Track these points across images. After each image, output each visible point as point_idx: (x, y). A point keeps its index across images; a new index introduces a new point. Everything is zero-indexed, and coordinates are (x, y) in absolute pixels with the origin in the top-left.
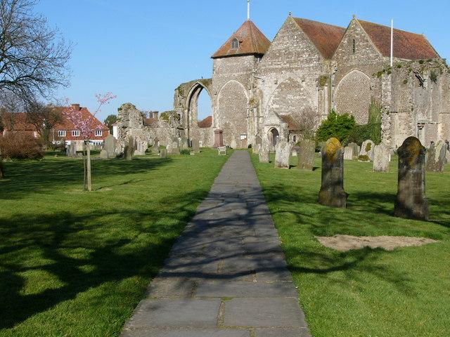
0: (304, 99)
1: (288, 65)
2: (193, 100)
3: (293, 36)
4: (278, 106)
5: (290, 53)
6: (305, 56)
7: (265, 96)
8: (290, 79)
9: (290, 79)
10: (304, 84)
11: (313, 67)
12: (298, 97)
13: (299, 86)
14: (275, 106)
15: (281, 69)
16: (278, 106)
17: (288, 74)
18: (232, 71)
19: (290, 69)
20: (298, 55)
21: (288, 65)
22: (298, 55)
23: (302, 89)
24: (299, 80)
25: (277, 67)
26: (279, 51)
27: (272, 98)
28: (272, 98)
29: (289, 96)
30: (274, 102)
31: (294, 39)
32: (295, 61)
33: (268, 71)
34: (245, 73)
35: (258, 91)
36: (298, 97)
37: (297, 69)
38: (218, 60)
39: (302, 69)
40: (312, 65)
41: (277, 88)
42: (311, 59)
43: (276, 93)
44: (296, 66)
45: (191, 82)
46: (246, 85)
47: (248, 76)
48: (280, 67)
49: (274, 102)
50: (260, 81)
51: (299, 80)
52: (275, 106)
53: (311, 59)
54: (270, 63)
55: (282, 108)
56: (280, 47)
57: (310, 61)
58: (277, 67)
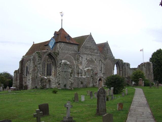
5: (91, 49)
6: (96, 51)
8: (91, 58)
9: (91, 58)
12: (93, 66)
13: (94, 62)
15: (88, 54)
20: (94, 50)
22: (94, 50)
24: (94, 60)
27: (85, 65)
28: (85, 65)
34: (74, 52)
35: (80, 61)
36: (93, 66)
37: (93, 55)
38: (62, 43)
39: (95, 55)
41: (87, 61)
42: (98, 53)
46: (74, 58)
50: (81, 58)
51: (94, 60)
54: (84, 51)
56: (88, 45)
57: (97, 53)
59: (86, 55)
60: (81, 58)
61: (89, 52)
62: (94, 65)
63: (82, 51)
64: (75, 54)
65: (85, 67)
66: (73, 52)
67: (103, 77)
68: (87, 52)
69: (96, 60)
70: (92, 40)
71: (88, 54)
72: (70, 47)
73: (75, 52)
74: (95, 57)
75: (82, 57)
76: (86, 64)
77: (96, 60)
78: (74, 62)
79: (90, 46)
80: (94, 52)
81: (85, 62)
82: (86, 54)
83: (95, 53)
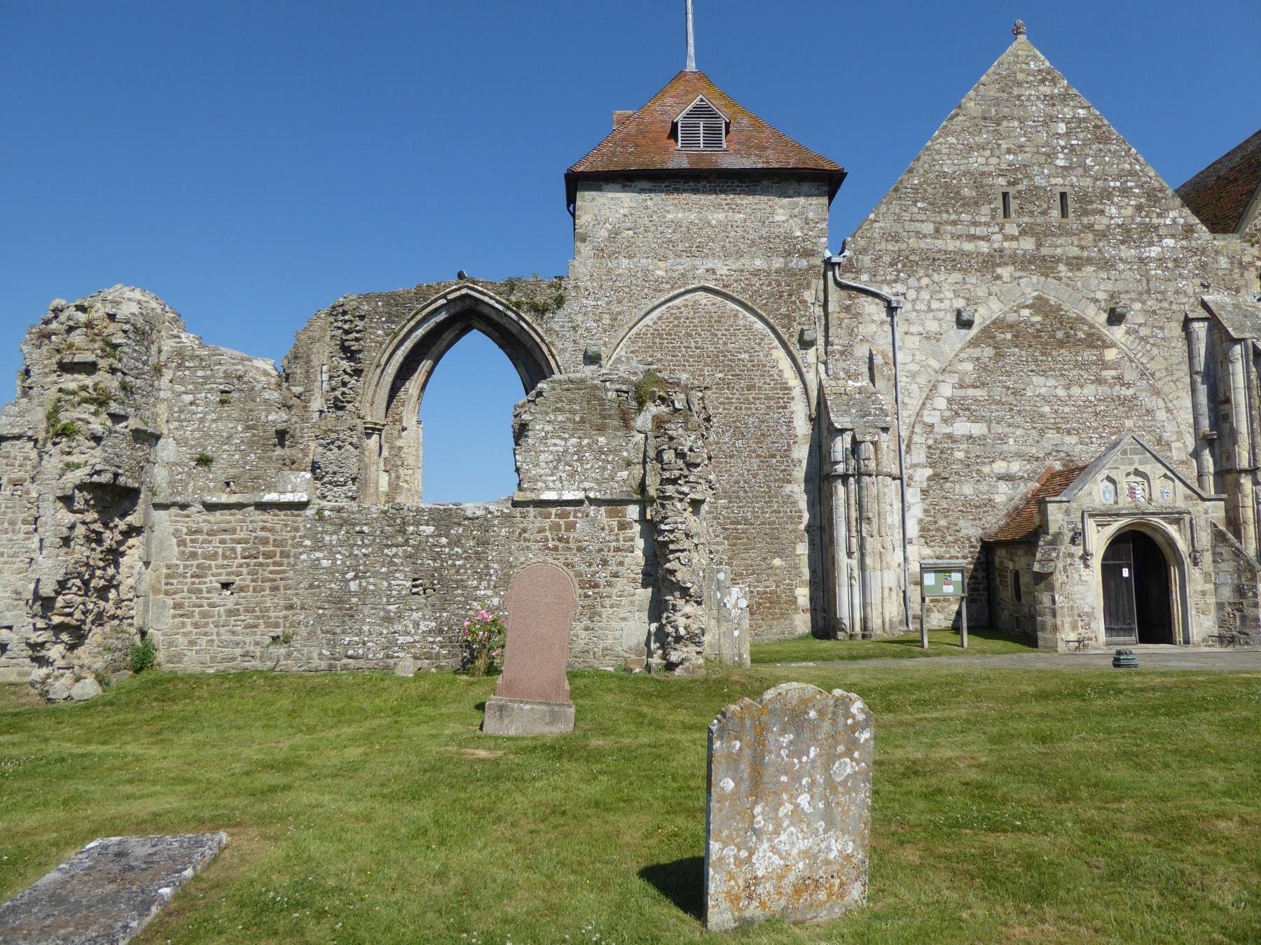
0: (1123, 401)
1: (1028, 244)
2: (412, 386)
3: (1053, 119)
4: (978, 429)
5: (1035, 191)
6: (1116, 213)
7: (903, 381)
8: (1040, 305)
9: (1040, 305)
10: (1118, 333)
11: (1161, 260)
12: (1090, 391)
13: (1095, 341)
14: (962, 427)
15: (990, 263)
16: (978, 429)
17: (1031, 286)
18: (696, 251)
19: (1045, 265)
21: (1028, 244)
23: (1111, 354)
25: (968, 246)
26: (978, 180)
28: (946, 390)
29: (1040, 385)
30: (959, 408)
31: (1059, 136)
32: (1064, 232)
33: (907, 264)
34: (778, 263)
37: (1076, 264)
39: (1106, 264)
40: (1154, 251)
41: (974, 343)
42: (1148, 229)
43: (968, 367)
44: (1075, 251)
45: (421, 294)
47: (798, 280)
48: (984, 247)
49: (959, 408)
52: (962, 427)
53: (1148, 229)
54: (928, 228)
55: (1002, 439)
56: (977, 161)
58: (968, 246)
59: (956, 276)
60: (874, 309)
61: (1013, 238)
62: (1099, 381)
63: (896, 238)
64: (798, 280)
65: (941, 403)
66: (759, 263)
67: (1176, 518)
68: (974, 238)
69: (1115, 318)
70: (1050, 100)
71: (990, 263)
72: (717, 217)
73: (788, 254)
74: (1099, 285)
75: (891, 310)
76: (963, 375)
77: (1115, 318)
78: (785, 364)
79: (1014, 173)
80: (1090, 227)
81: (935, 355)
82: (954, 262)
83: (1103, 235)
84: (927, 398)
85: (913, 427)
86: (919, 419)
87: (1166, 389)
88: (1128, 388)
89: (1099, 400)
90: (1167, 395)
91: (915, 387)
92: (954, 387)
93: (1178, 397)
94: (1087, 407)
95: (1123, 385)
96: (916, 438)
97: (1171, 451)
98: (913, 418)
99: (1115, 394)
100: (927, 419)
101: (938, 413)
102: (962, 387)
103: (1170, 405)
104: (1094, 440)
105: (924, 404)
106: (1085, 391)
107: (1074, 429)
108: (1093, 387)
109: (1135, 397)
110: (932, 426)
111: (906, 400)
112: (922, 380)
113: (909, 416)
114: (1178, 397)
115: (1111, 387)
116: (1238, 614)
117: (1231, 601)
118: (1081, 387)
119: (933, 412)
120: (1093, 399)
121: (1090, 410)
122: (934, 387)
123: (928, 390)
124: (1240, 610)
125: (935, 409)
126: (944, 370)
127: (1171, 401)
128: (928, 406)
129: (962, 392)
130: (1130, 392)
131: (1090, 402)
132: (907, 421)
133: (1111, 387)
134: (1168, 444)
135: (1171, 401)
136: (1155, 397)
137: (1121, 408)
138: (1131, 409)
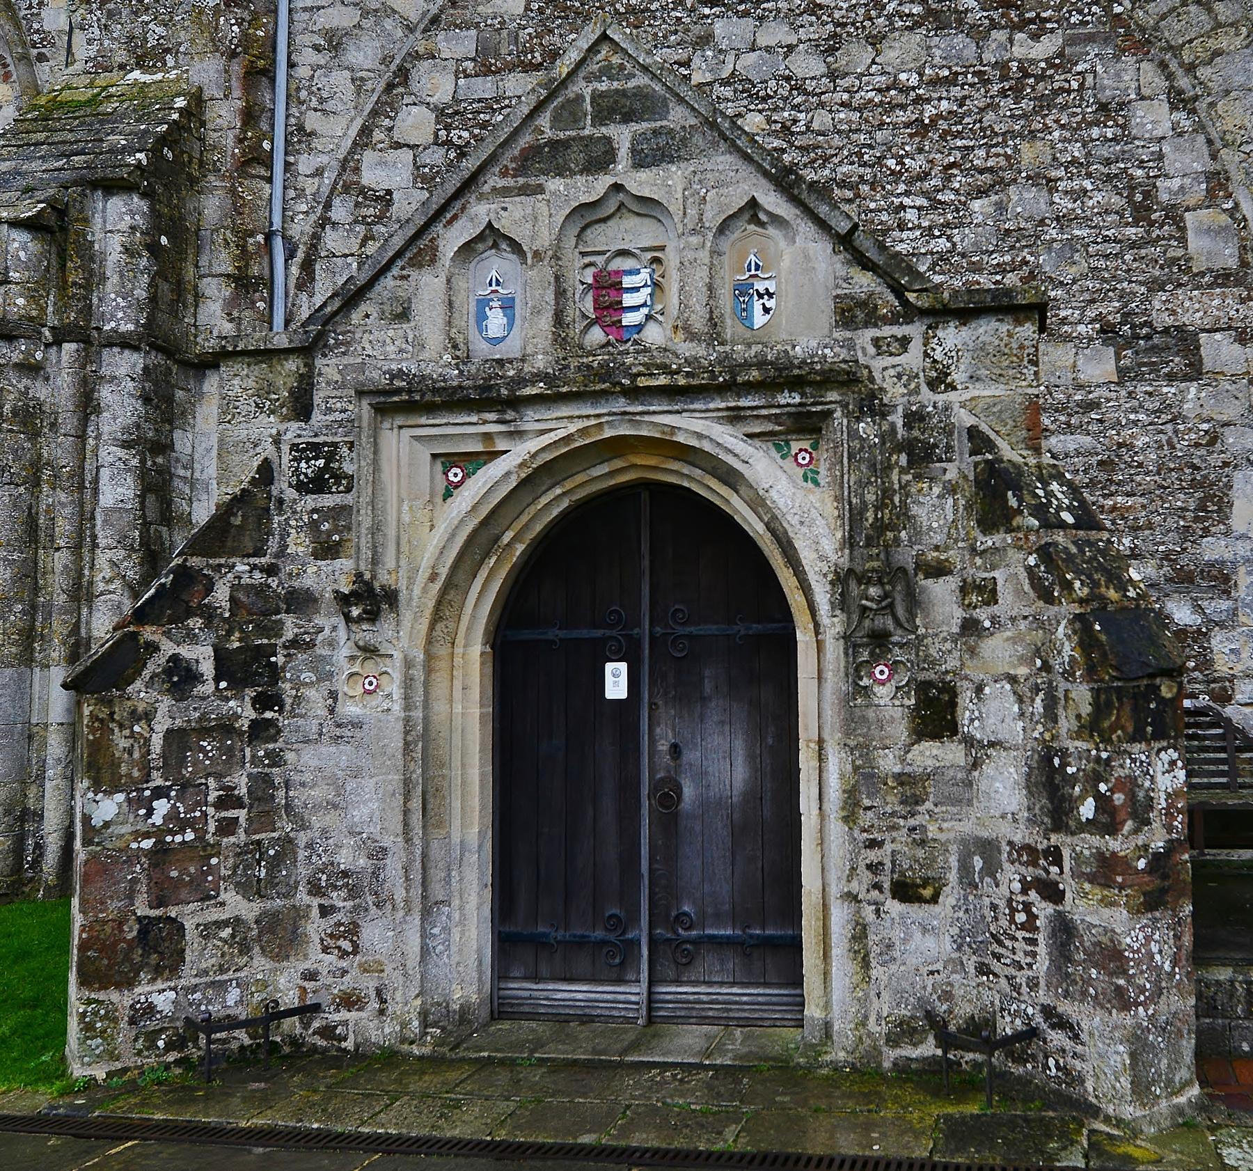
84: (374, 113)
85: (328, 206)
86: (348, 177)
87: (1173, 31)
88: (1035, 37)
89: (935, 82)
90: (1175, 50)
91: (341, 79)
92: (460, 73)
93: (1217, 53)
94: (892, 107)
95: (1022, 25)
96: (332, 240)
97: (1183, 240)
98: (329, 178)
99: (989, 57)
100: (373, 175)
101: (407, 155)
102: (486, 70)
103: (1183, 82)
104: (911, 215)
105: (366, 131)
106: (891, 54)
107: (843, 184)
108: (917, 37)
109: (1061, 62)
110: (386, 199)
111: (313, 121)
112: (363, 55)
113: (319, 172)
114: (1217, 53)
115: (979, 35)
116: (1044, 910)
117: (1020, 836)
118: (875, 41)
119: (392, 155)
120: (914, 80)
121: (901, 116)
122: (403, 74)
123: (381, 86)
124: (1052, 893)
125: (398, 146)
126: (435, 20)
127: (1190, 69)
128: (378, 135)
129: (484, 87)
130: (1046, 47)
131: (904, 90)
132: (310, 186)
133: (979, 35)
134: (1174, 215)
135: (1190, 69)
136: (1128, 59)
137: (1007, 104)
138: (1045, 104)
